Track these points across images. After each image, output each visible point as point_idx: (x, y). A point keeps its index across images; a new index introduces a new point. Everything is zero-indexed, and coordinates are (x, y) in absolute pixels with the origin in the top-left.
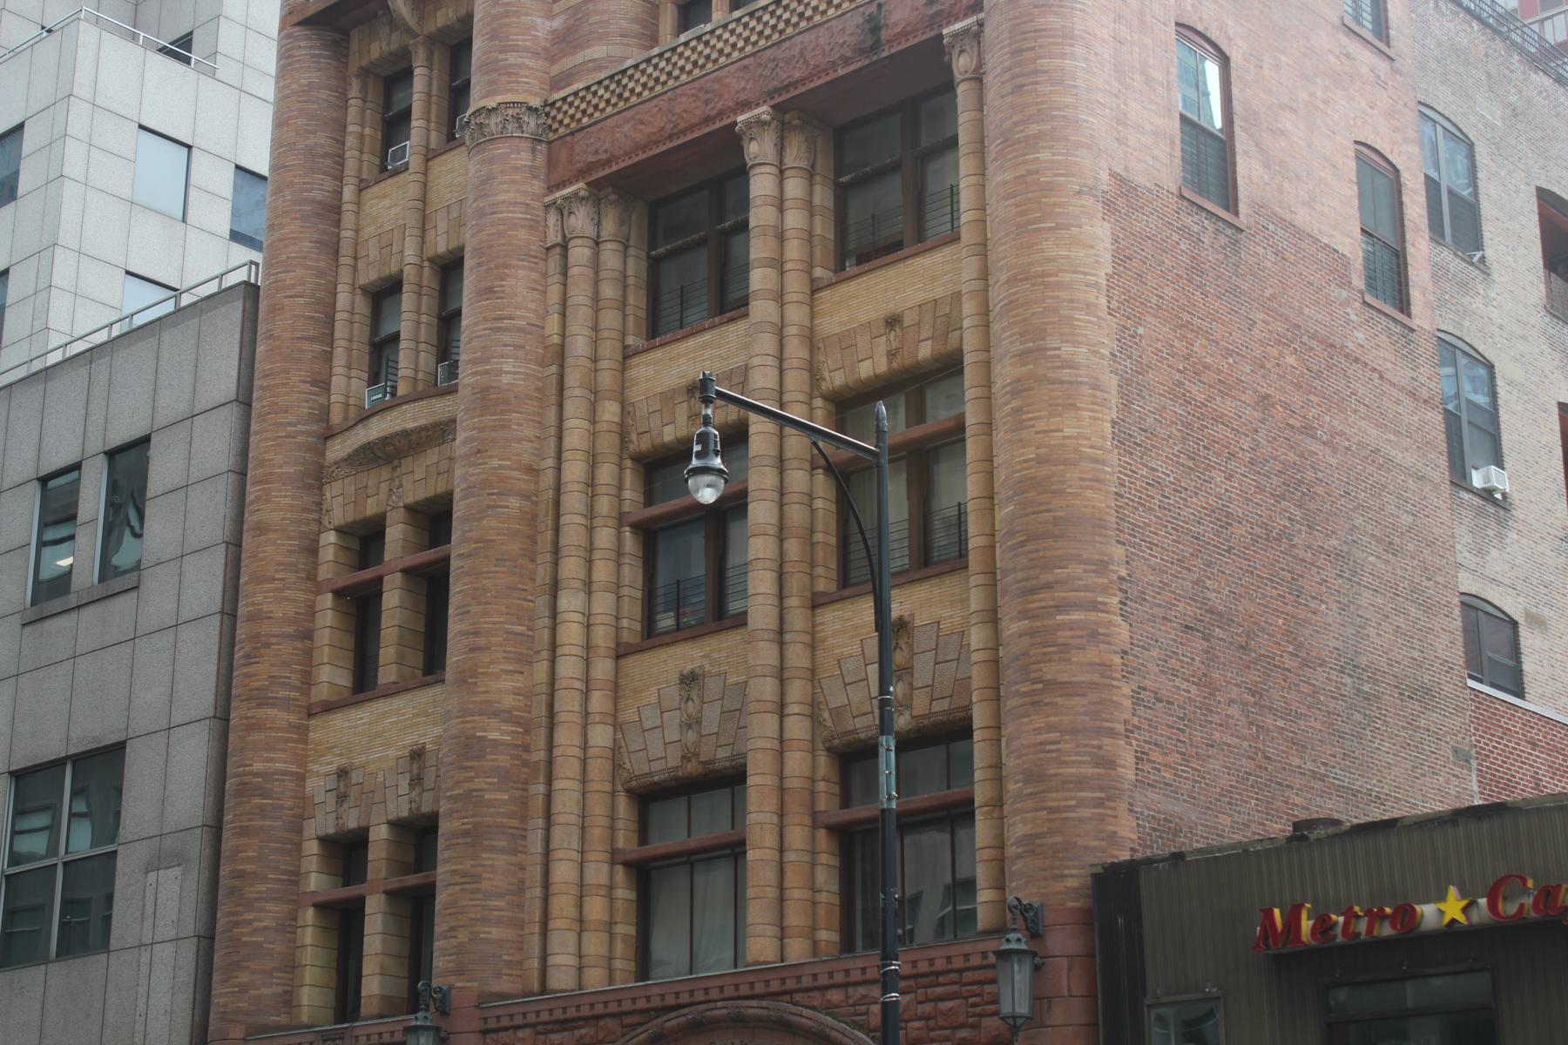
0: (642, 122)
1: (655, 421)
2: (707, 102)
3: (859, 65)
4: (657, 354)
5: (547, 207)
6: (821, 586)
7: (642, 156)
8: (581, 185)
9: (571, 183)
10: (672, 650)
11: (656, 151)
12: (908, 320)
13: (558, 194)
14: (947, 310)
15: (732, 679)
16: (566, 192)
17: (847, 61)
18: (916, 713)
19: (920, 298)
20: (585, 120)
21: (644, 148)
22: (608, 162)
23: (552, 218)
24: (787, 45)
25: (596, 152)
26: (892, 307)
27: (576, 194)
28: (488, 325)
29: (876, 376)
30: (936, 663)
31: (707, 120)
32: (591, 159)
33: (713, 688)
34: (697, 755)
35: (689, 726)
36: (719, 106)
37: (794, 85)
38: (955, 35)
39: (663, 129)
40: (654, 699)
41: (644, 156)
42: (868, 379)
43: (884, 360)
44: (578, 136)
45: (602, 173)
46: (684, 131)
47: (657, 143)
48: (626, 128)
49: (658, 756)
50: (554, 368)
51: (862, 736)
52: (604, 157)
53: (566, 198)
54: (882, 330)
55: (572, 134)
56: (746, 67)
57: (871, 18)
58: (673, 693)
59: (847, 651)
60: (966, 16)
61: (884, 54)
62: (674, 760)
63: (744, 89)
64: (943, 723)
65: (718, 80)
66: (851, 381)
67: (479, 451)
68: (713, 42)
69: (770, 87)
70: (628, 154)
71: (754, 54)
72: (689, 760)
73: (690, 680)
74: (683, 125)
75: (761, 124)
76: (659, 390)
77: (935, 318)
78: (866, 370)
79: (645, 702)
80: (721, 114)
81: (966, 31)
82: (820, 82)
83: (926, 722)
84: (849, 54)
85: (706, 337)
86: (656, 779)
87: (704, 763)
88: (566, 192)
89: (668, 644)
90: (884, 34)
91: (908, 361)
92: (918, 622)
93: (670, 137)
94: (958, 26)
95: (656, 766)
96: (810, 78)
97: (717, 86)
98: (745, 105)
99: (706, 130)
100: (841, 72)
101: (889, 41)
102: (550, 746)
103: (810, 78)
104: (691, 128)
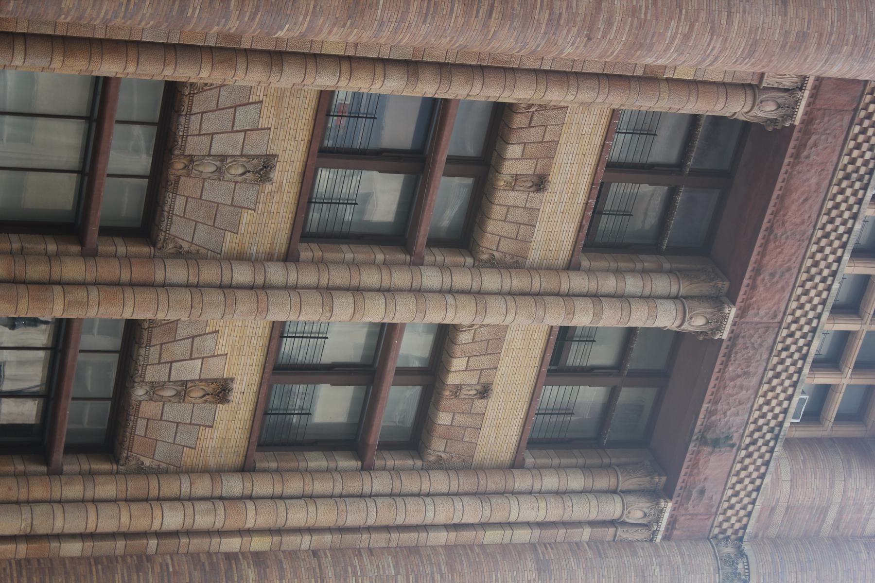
0: (806, 200)
1: (534, 134)
2: (772, 275)
3: (699, 423)
4: (591, 161)
5: (804, 78)
6: (288, 346)
7: (776, 193)
8: (725, 336)
9: (809, 104)
10: (303, 147)
11: (770, 209)
12: (479, 404)
13: (807, 94)
14: (466, 439)
15: (246, 216)
16: (803, 103)
17: (711, 413)
18: (143, 404)
19: (490, 414)
20: (857, 129)
21: (782, 198)
22: (797, 156)
23: (787, 83)
24: (765, 356)
25: (815, 145)
26: (497, 389)
27: (792, 116)
28: (715, 52)
29: (448, 371)
30: (178, 423)
31: (758, 271)
32: (814, 138)
33: (246, 194)
34: (188, 175)
35: (218, 170)
36: (761, 289)
37: (725, 364)
38: (661, 511)
39: (783, 224)
40: (264, 123)
41: (774, 196)
42: (449, 363)
43: (457, 382)
44: (847, 119)
45: (792, 144)
46: (765, 246)
47: (775, 214)
48: (814, 180)
49: (205, 132)
50: (639, 72)
51: (142, 352)
52: (805, 153)
53: (797, 102)
54: (482, 381)
55: (856, 110)
56: (775, 316)
57: (729, 437)
58: (257, 146)
59: (222, 341)
60: (671, 516)
61: (692, 445)
62: (194, 145)
63: (757, 315)
64: (126, 426)
65: (783, 289)
66: (458, 350)
67: (589, 39)
68: (821, 286)
69: (741, 341)
70: (787, 181)
71: (781, 323)
72: (186, 167)
73: (264, 168)
74: (772, 245)
75: (719, 328)
76: (562, 141)
77: (465, 428)
78: (458, 363)
79: (265, 110)
80: (753, 287)
81: (658, 521)
82: (711, 385)
83: (132, 412)
84: (713, 418)
85: (581, 198)
86: (182, 120)
87: (177, 182)
88: (803, 103)
89: (310, 142)
90: (707, 449)
91: (444, 403)
92: (220, 406)
93: (770, 230)
94: (666, 516)
95: (195, 120)
96: (720, 379)
97: (779, 286)
98: (742, 313)
99: (750, 268)
100: (705, 406)
101: (699, 452)
102: (250, 54)
103: (720, 379)
104: (762, 254)
